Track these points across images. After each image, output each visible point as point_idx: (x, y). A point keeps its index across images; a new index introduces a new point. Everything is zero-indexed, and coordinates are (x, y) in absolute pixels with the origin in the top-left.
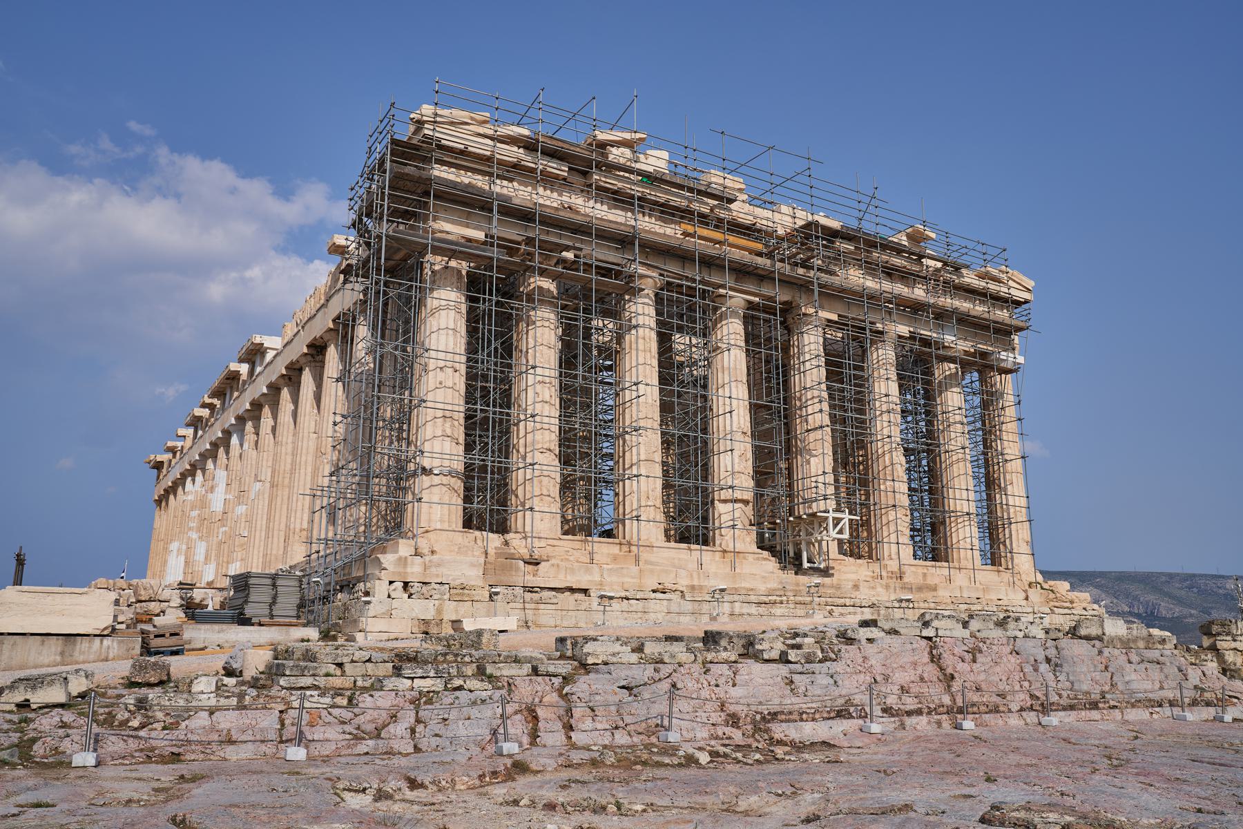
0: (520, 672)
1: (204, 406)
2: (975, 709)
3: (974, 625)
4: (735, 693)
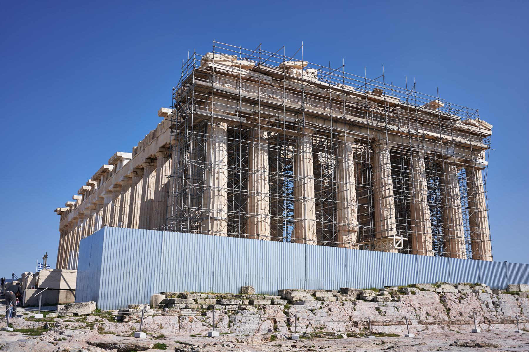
0: (267, 303)
2: (459, 323)
3: (460, 287)
4: (355, 313)
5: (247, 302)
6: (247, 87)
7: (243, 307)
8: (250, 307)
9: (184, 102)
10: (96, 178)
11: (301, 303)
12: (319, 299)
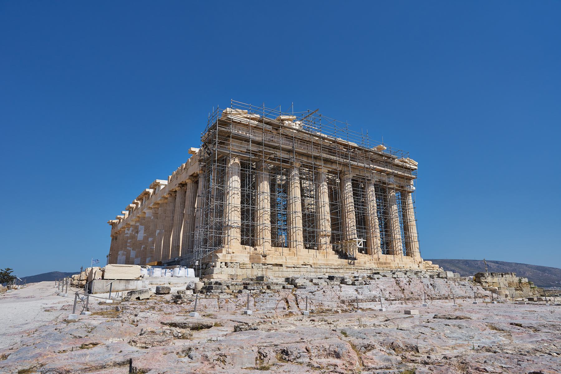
1: (134, 203)
5: (265, 287)
6: (254, 132)
7: (264, 291)
8: (268, 291)
9: (210, 143)
10: (141, 199)
11: (303, 287)
12: (315, 284)
